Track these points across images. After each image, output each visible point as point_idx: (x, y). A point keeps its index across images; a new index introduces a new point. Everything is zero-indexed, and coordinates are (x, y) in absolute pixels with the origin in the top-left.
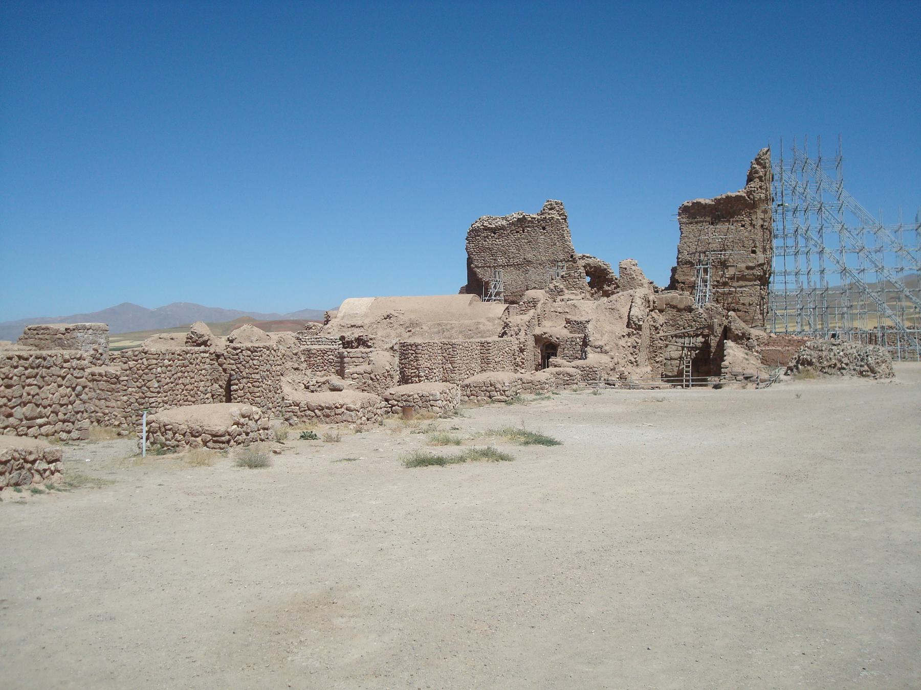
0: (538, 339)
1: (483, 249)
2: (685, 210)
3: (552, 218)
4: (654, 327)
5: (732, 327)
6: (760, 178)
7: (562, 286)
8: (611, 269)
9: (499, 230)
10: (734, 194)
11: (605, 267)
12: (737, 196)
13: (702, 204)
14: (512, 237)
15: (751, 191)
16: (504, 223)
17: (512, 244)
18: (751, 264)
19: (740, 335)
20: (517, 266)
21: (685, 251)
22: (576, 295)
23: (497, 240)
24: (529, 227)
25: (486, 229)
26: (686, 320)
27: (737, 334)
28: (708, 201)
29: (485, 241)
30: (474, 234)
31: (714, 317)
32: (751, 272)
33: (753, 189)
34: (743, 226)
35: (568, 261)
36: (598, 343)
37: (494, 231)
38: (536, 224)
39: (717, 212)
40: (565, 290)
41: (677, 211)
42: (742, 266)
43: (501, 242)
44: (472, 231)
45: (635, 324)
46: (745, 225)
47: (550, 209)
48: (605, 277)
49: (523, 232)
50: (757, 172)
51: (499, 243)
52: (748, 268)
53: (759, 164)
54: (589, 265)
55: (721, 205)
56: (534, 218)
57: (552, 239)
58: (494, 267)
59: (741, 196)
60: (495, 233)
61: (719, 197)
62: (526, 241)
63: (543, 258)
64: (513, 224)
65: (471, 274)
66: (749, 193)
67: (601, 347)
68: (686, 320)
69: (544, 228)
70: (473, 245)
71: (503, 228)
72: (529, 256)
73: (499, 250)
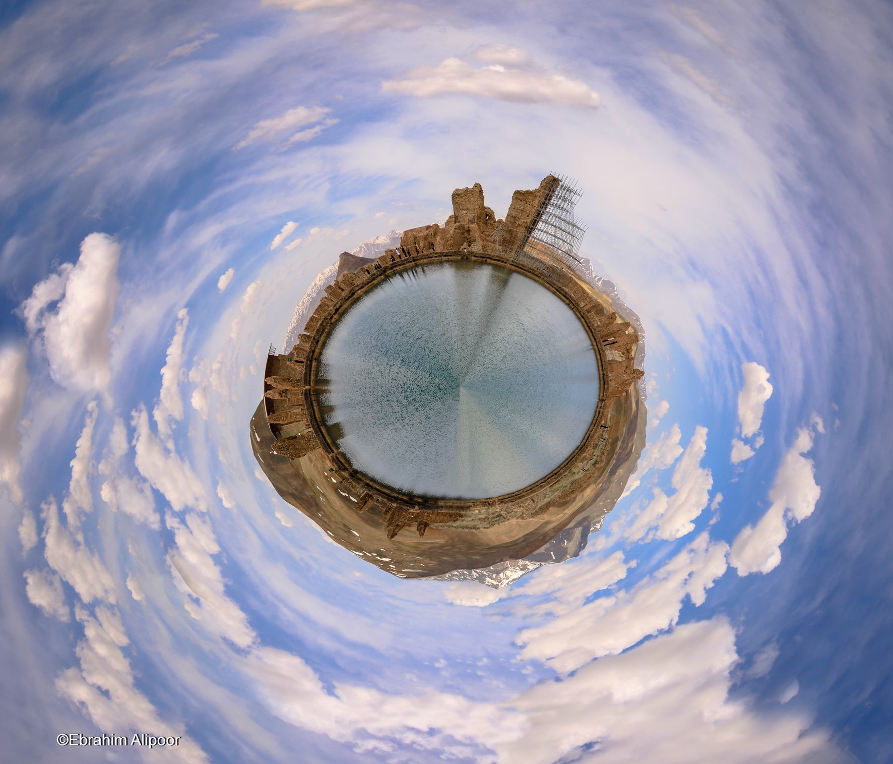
18: (525, 221)
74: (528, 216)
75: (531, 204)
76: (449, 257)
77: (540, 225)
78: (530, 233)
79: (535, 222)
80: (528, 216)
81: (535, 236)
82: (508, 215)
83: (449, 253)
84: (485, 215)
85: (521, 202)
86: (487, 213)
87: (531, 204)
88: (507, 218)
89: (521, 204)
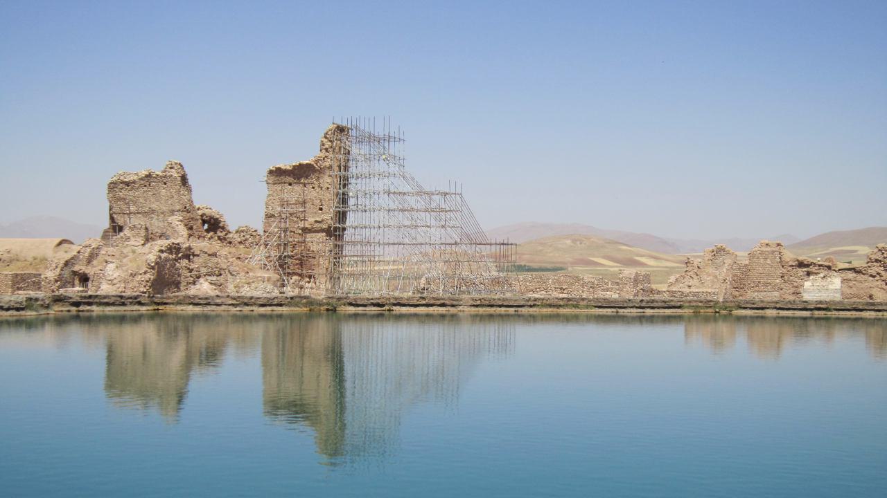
0: (75, 273)
1: (120, 199)
2: (271, 172)
3: (172, 175)
6: (326, 150)
7: (128, 235)
9: (132, 183)
10: (305, 162)
11: (218, 216)
12: (307, 164)
14: (142, 190)
16: (136, 178)
18: (318, 219)
20: (145, 214)
24: (154, 182)
25: (123, 182)
28: (288, 168)
30: (113, 186)
32: (318, 225)
34: (313, 188)
35: (183, 211)
37: (127, 184)
41: (266, 174)
42: (312, 220)
44: (111, 183)
47: (171, 168)
50: (323, 145)
52: (316, 222)
53: (326, 137)
54: (204, 214)
58: (128, 214)
59: (310, 164)
60: (128, 186)
61: (294, 164)
63: (164, 208)
64: (142, 179)
65: (112, 219)
67: (112, 280)
69: (165, 184)
71: (134, 182)
72: (153, 206)
73: (131, 200)
74: (321, 209)
75: (316, 186)
76: (275, 308)
77: (351, 219)
78: (341, 237)
79: (342, 216)
80: (321, 209)
81: (347, 240)
82: (269, 216)
83: (276, 300)
84: (200, 221)
85: (290, 187)
86: (204, 217)
87: (316, 186)
88: (267, 224)
89: (293, 193)
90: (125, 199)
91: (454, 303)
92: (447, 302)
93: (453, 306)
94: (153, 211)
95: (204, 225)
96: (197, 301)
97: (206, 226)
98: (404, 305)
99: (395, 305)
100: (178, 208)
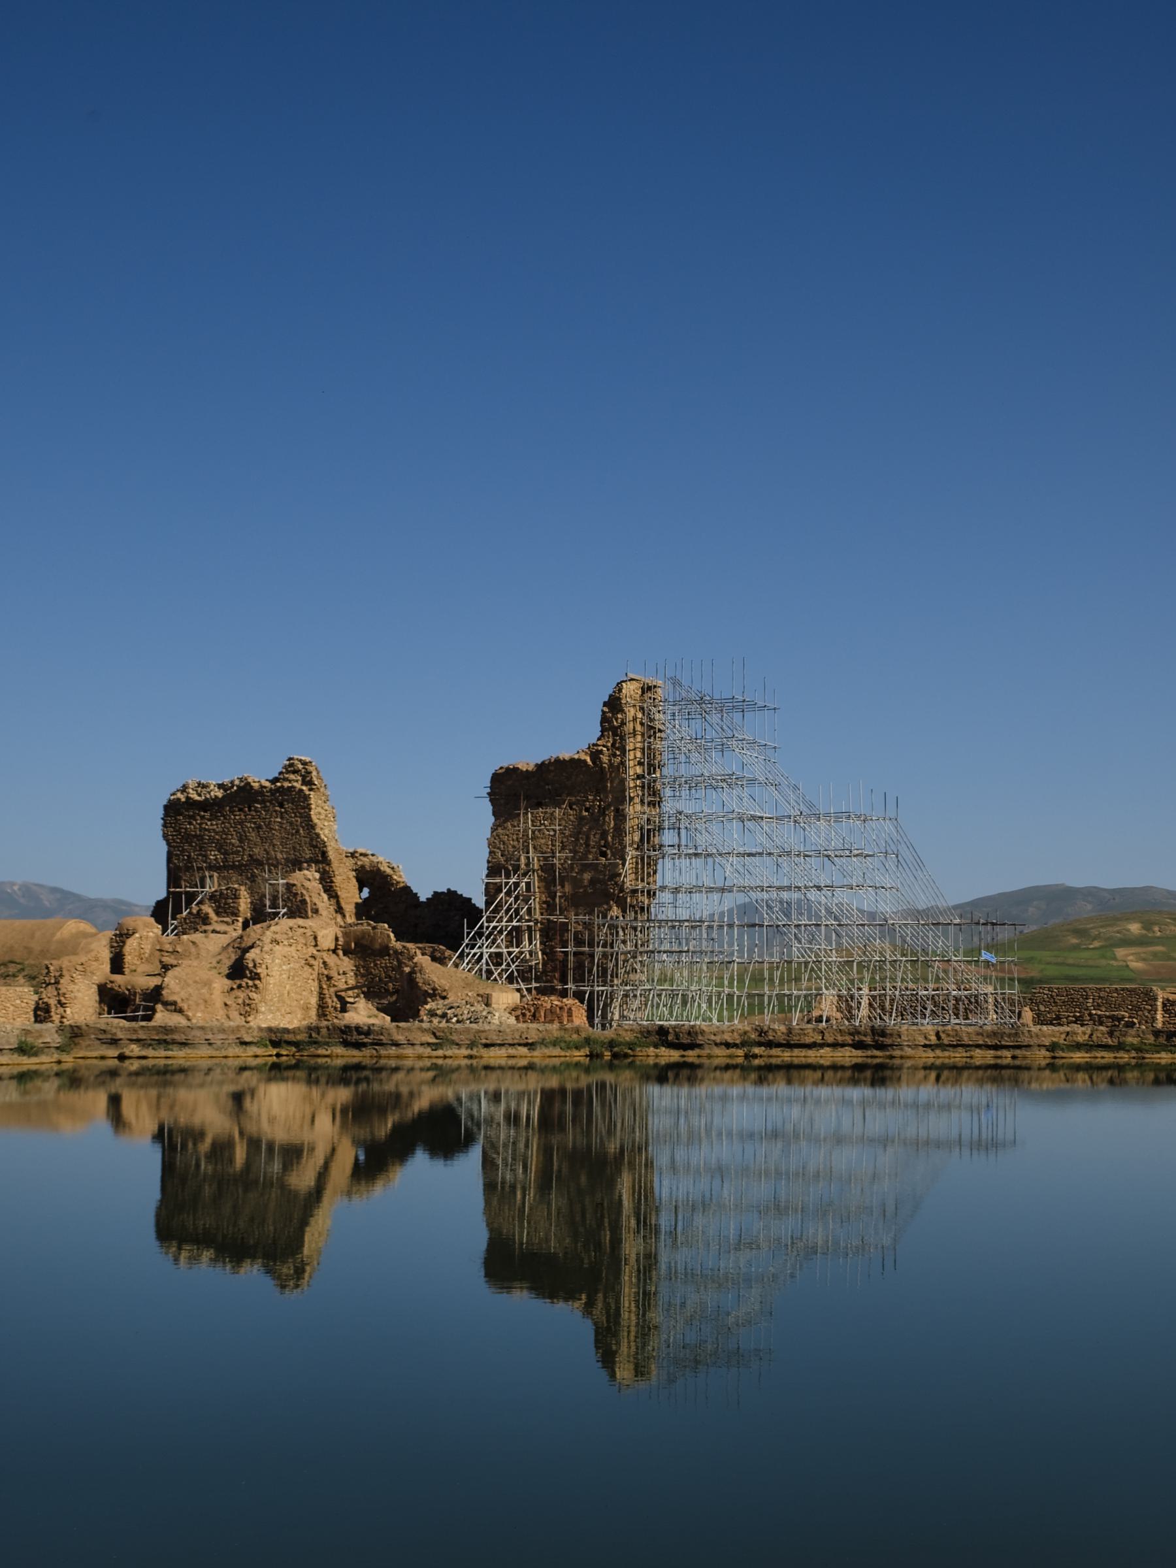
1: (188, 838)
3: (293, 787)
4: (327, 976)
5: (417, 980)
8: (400, 877)
10: (566, 755)
11: (389, 871)
13: (522, 771)
15: (597, 750)
16: (220, 794)
17: (232, 829)
19: (431, 991)
21: (498, 851)
22: (227, 923)
23: (209, 823)
25: (190, 803)
26: (381, 967)
27: (426, 991)
29: (190, 823)
30: (174, 810)
31: (405, 963)
33: (600, 748)
36: (171, 998)
37: (205, 805)
38: (267, 796)
39: (548, 785)
40: (212, 915)
43: (215, 827)
45: (251, 972)
46: (590, 808)
48: (390, 890)
49: (250, 810)
51: (211, 827)
55: (552, 774)
56: (265, 787)
57: (291, 824)
62: (253, 826)
63: (279, 856)
65: (173, 878)
66: (595, 755)
68: (381, 967)
69: (281, 806)
70: (172, 830)
73: (211, 839)
90: (200, 838)
91: (888, 1041)
92: (868, 1040)
93: (881, 1047)
94: (260, 864)
95: (361, 890)
96: (355, 1037)
97: (366, 892)
98: (779, 1045)
99: (760, 1044)
100: (308, 854)
